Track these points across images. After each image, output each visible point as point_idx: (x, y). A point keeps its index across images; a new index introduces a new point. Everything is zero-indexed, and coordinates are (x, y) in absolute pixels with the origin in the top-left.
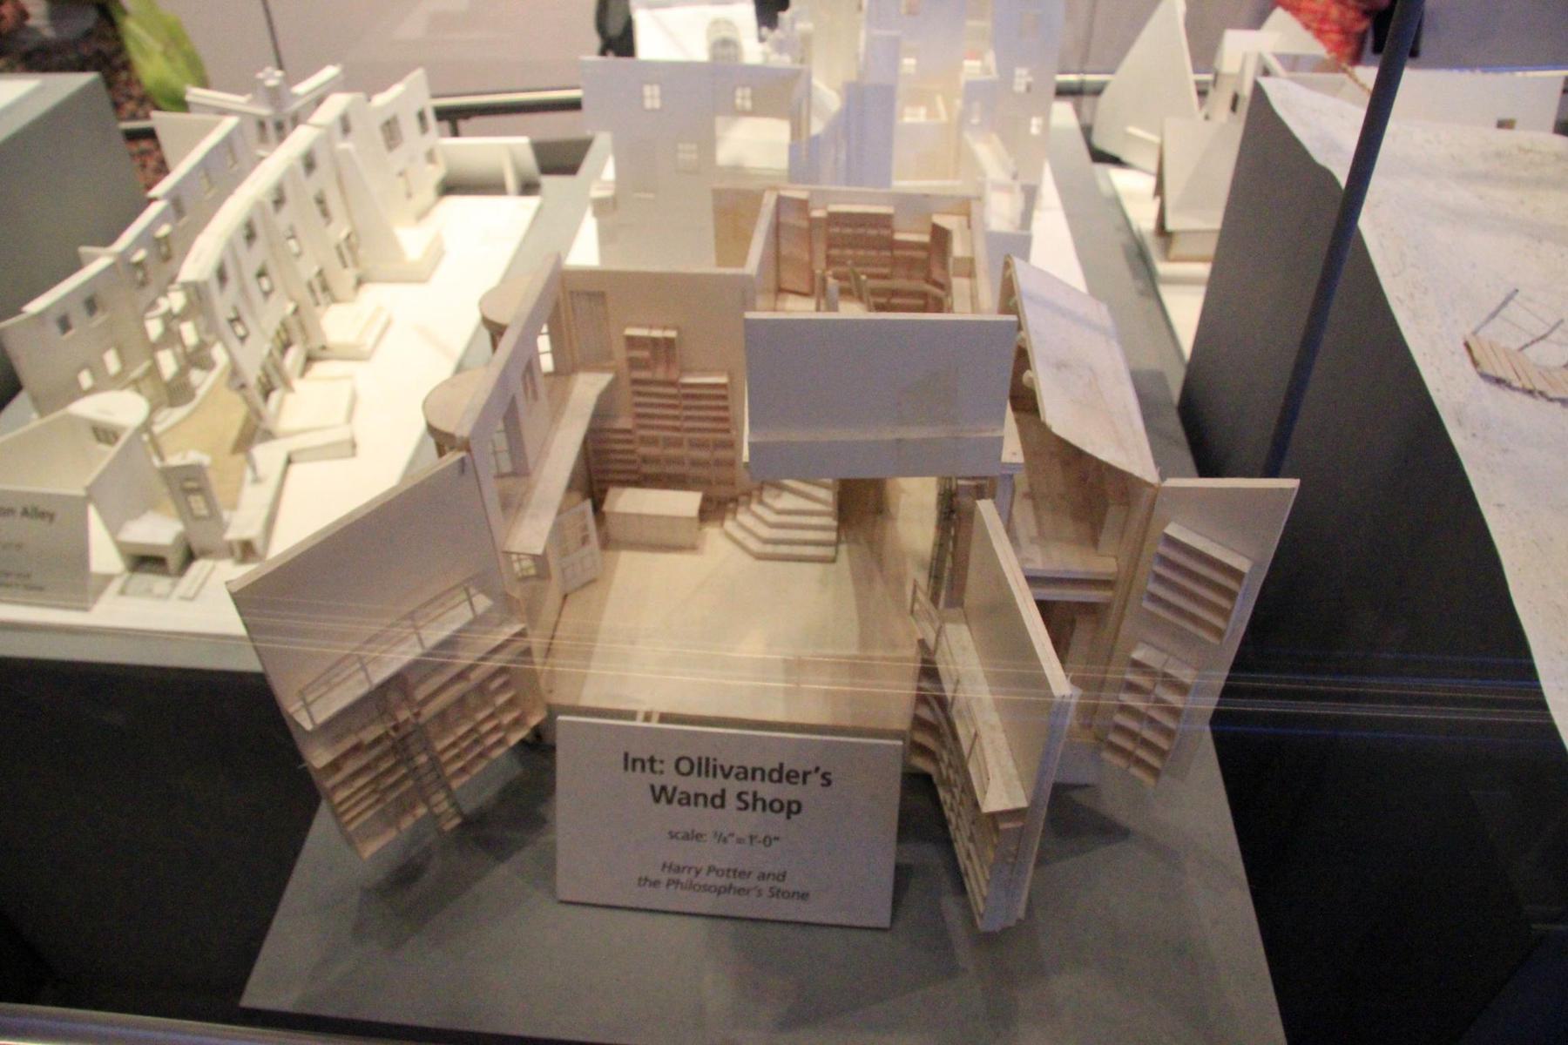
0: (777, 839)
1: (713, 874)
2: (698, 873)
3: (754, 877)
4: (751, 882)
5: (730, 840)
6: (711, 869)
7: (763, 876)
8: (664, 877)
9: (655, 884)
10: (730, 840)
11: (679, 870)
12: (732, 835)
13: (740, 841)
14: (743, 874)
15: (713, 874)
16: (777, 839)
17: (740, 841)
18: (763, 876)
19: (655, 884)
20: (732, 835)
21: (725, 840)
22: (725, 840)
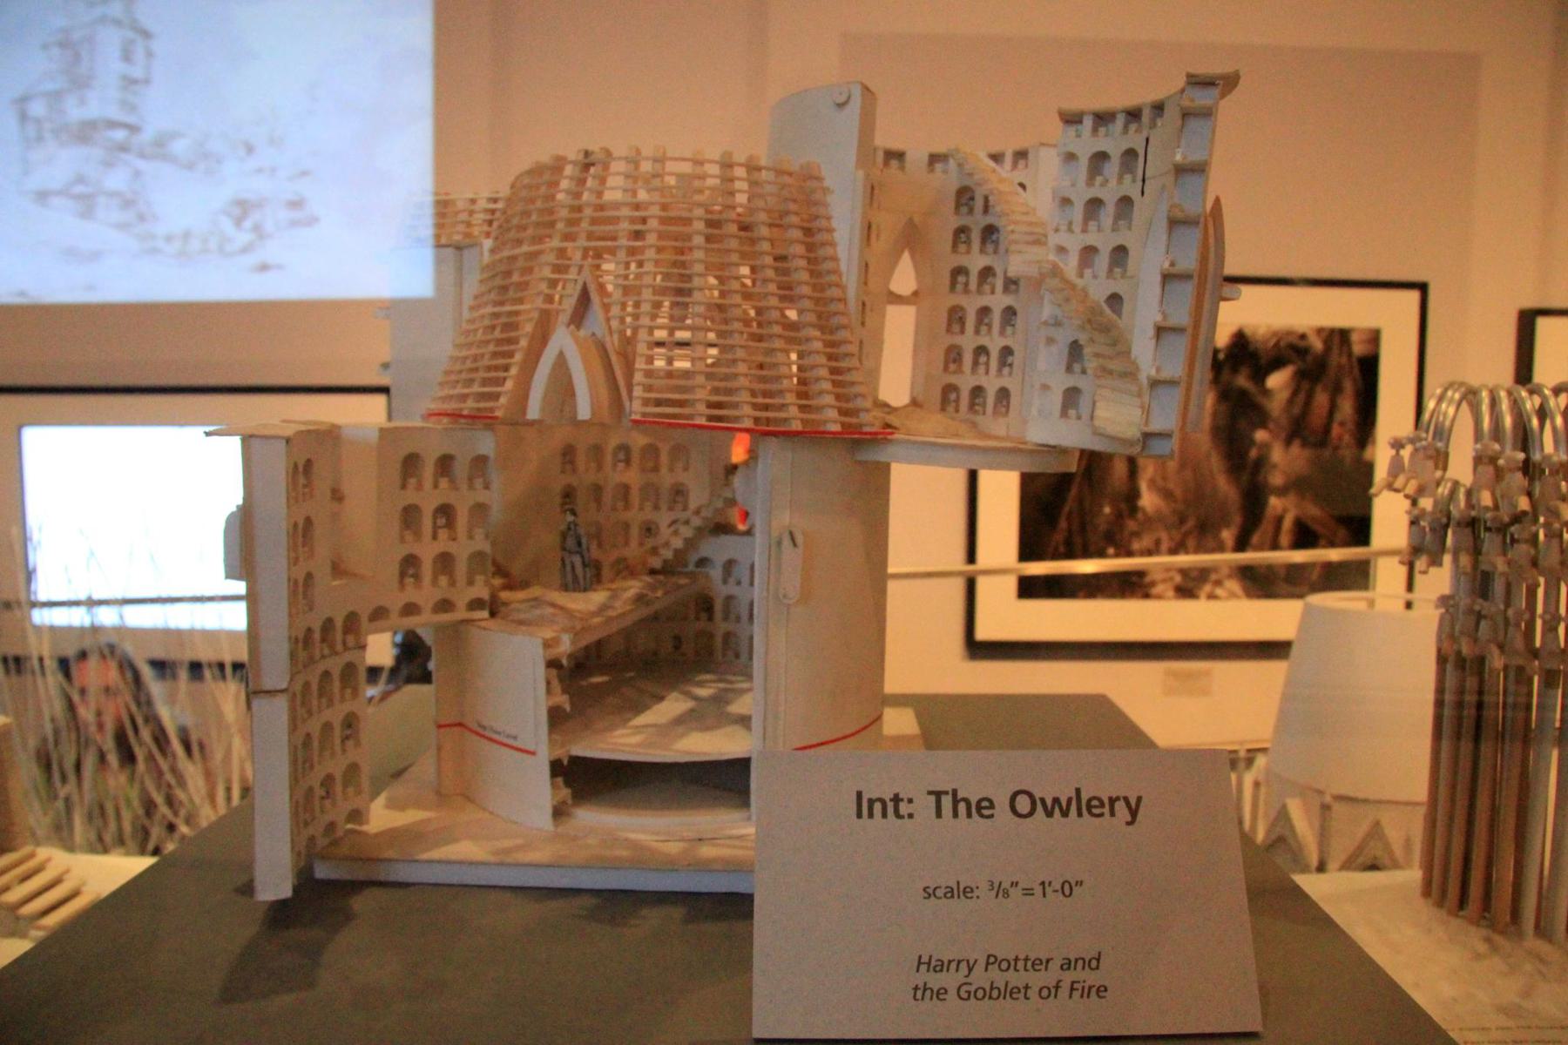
1: (994, 969)
2: (970, 970)
3: (1055, 966)
5: (1012, 891)
6: (991, 960)
7: (1067, 965)
10: (1012, 891)
11: (941, 967)
12: (1014, 884)
13: (1028, 892)
14: (1038, 964)
15: (994, 969)
17: (1028, 892)
18: (1067, 965)
21: (1006, 894)
22: (1006, 894)
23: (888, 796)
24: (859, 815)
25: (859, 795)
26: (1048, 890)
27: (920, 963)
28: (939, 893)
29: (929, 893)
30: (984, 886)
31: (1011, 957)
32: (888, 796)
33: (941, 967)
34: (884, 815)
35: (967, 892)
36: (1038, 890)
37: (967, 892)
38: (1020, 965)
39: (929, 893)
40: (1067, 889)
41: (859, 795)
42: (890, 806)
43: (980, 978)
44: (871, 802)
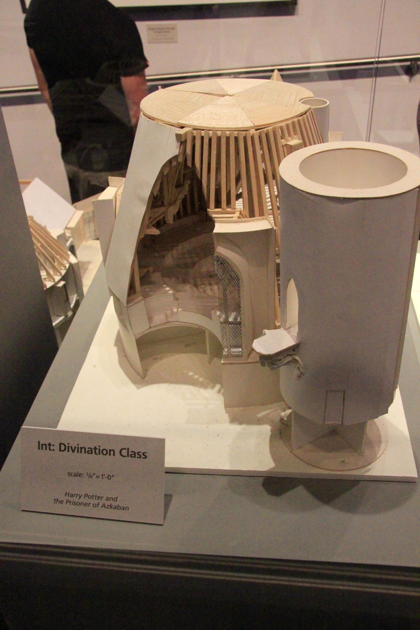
0: (113, 476)
1: (86, 498)
2: (80, 497)
4: (103, 501)
6: (86, 495)
7: (108, 499)
8: (65, 499)
9: (61, 502)
11: (72, 496)
12: (94, 474)
13: (98, 477)
16: (113, 476)
17: (98, 477)
18: (108, 499)
19: (61, 502)
20: (94, 474)
21: (91, 477)
22: (91, 477)
23: (47, 444)
24: (39, 449)
25: (39, 442)
26: (104, 477)
27: (66, 494)
28: (72, 475)
29: (70, 474)
30: (85, 474)
31: (92, 495)
32: (47, 444)
33: (72, 496)
34: (46, 449)
35: (80, 475)
36: (101, 477)
37: (80, 475)
38: (94, 497)
39: (70, 474)
40: (109, 477)
41: (39, 442)
42: (48, 446)
43: (81, 500)
44: (42, 445)
